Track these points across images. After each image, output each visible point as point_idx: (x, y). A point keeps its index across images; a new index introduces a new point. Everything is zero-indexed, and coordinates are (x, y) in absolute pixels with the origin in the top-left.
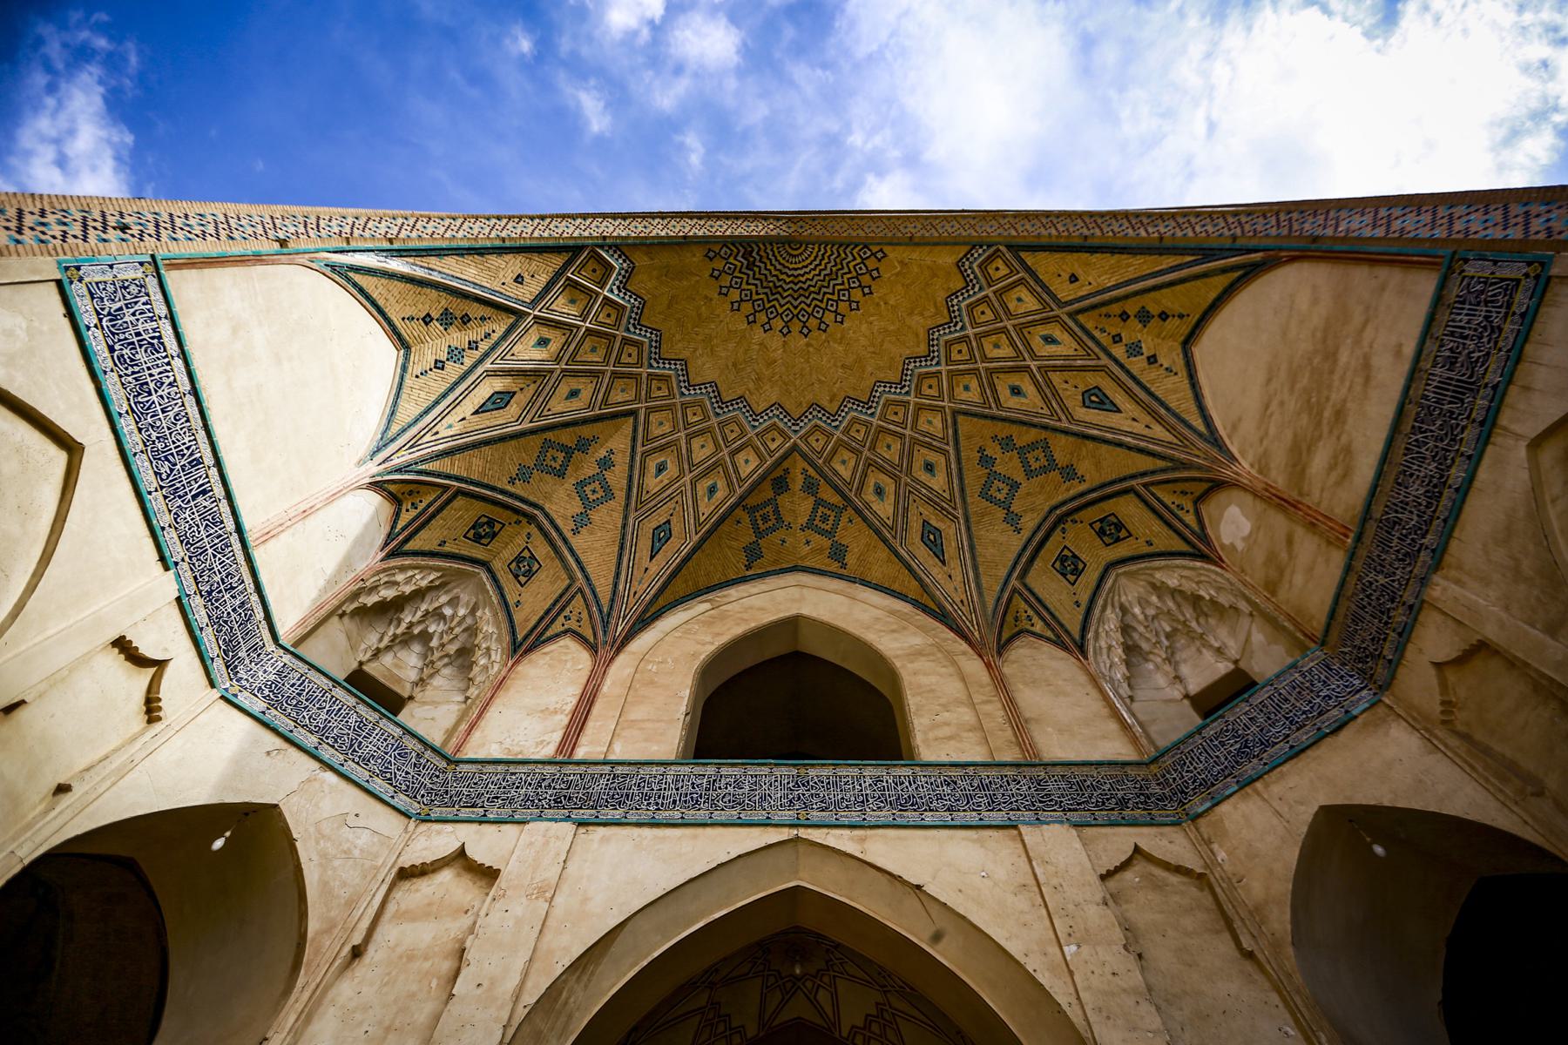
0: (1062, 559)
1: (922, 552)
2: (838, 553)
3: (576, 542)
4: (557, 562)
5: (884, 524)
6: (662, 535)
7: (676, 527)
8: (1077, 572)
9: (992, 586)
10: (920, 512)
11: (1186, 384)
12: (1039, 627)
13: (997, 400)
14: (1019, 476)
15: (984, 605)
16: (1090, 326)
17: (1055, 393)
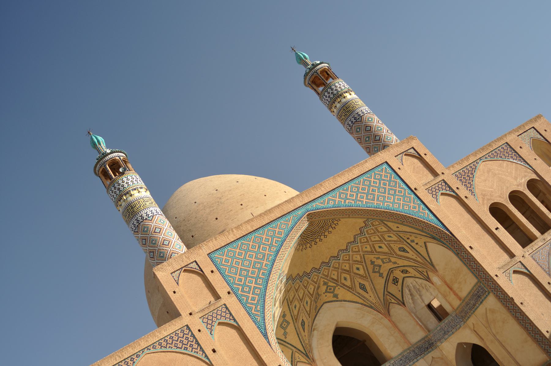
0: (394, 280)
1: (361, 291)
2: (336, 296)
3: (287, 340)
4: (286, 348)
5: (350, 288)
7: (305, 320)
8: (397, 282)
9: (381, 296)
10: (358, 280)
11: (425, 250)
12: (393, 301)
13: (375, 250)
14: (381, 263)
15: (381, 302)
16: (401, 235)
17: (392, 248)
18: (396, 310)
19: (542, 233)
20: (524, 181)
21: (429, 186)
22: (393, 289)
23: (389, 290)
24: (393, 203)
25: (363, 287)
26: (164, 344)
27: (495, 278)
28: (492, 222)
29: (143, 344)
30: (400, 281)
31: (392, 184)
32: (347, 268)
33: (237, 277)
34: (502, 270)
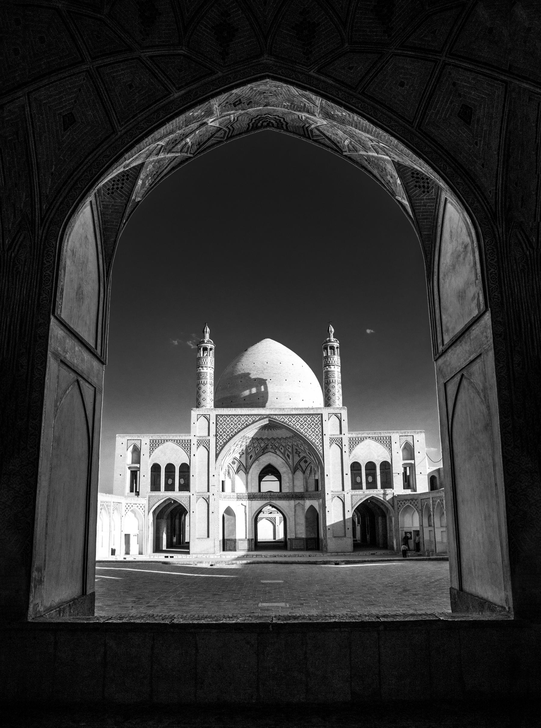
1: (287, 457)
6: (251, 457)
18: (299, 474)
19: (367, 488)
20: (382, 460)
21: (333, 436)
22: (302, 464)
23: (301, 463)
24: (310, 435)
25: (288, 456)
26: (178, 442)
27: (326, 494)
28: (347, 470)
29: (171, 438)
30: (308, 463)
31: (317, 426)
32: (284, 445)
33: (221, 430)
34: (332, 493)
